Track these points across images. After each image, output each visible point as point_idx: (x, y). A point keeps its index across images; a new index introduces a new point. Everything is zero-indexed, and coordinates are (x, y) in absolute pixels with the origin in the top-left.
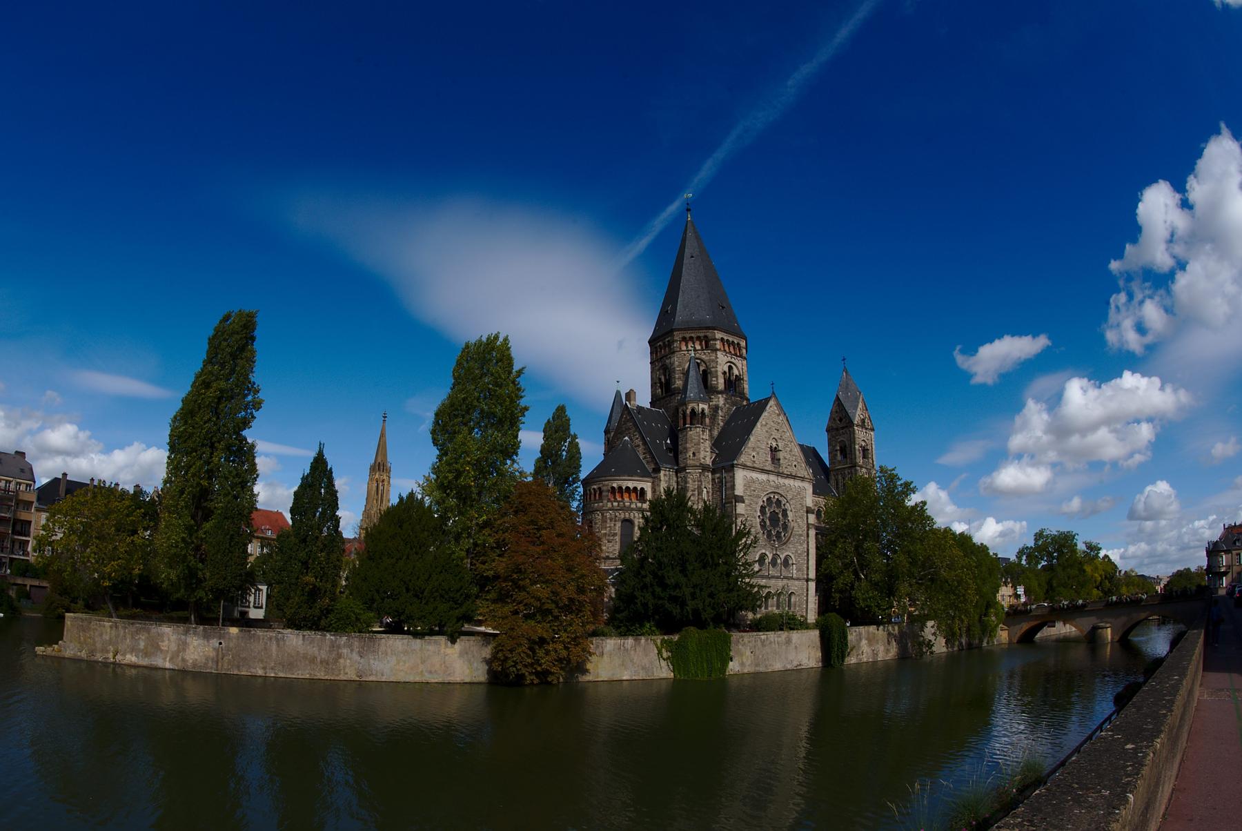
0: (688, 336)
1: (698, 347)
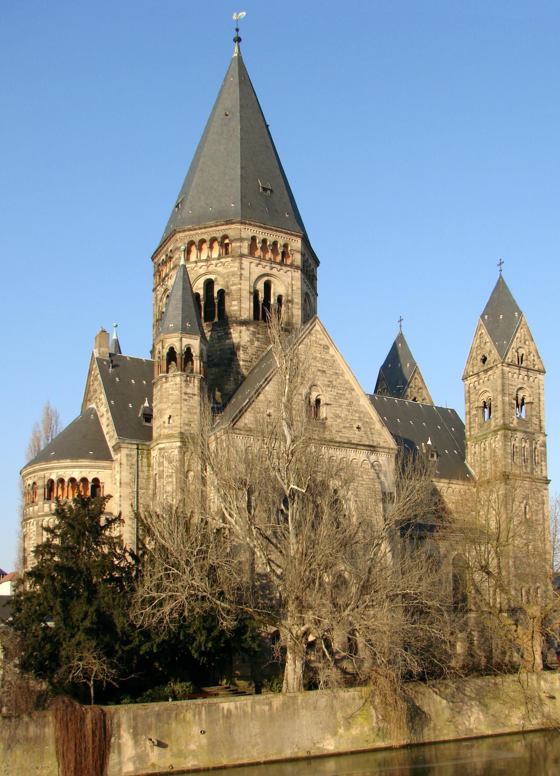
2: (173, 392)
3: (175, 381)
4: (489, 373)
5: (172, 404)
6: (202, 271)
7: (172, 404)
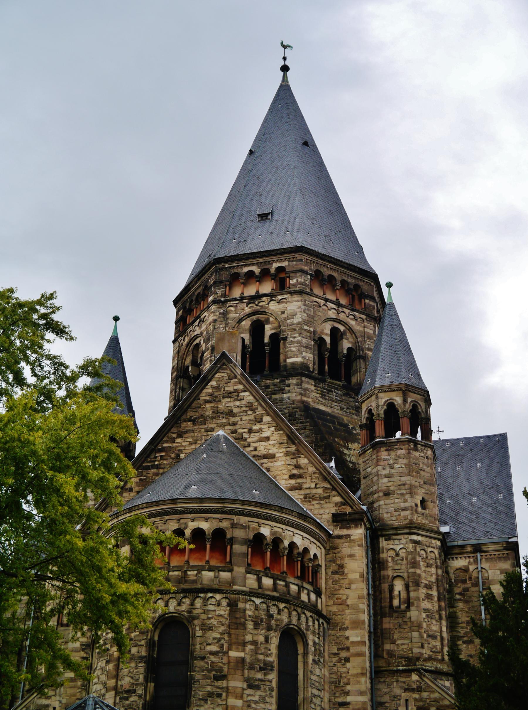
0: (326, 272)
2: (425, 467)
3: (426, 453)
5: (425, 483)
6: (332, 314)
7: (425, 483)
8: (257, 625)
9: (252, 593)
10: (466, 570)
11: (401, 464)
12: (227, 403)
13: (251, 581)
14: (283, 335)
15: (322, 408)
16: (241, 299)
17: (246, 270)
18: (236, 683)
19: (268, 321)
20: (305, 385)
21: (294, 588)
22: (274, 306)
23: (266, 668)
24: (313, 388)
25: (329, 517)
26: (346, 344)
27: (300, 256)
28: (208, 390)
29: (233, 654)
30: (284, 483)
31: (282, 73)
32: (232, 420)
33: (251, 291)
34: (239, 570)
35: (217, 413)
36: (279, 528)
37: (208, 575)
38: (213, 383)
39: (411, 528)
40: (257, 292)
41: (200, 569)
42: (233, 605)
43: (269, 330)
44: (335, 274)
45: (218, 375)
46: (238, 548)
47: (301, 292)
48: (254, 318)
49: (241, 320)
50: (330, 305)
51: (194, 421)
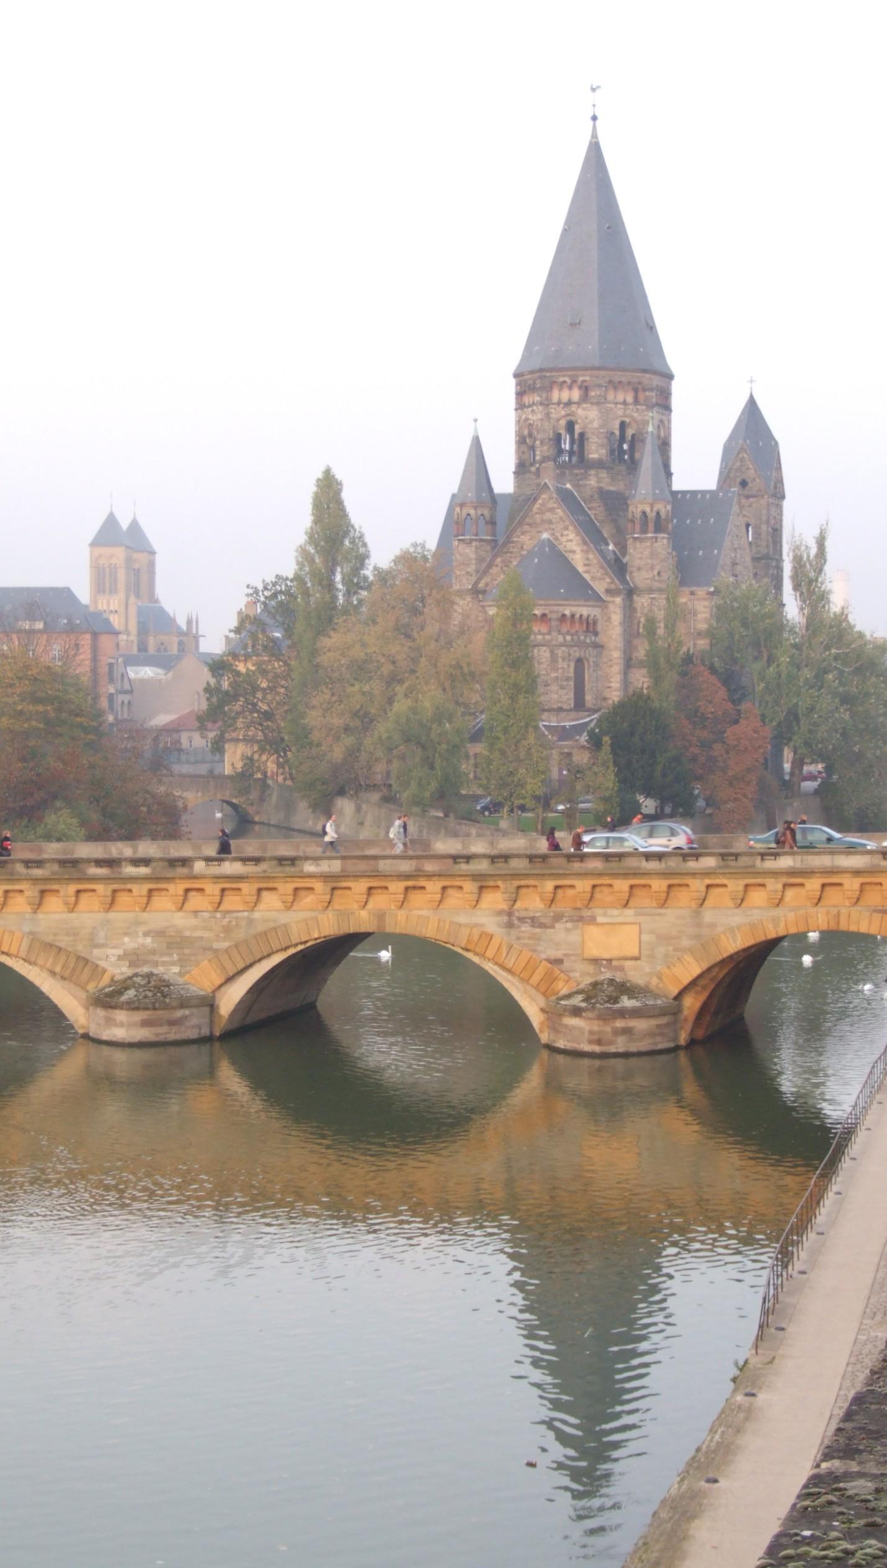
0: (616, 379)
1: (630, 399)
4: (751, 500)
6: (620, 413)
8: (563, 660)
9: (561, 645)
10: (686, 604)
11: (647, 552)
12: (548, 516)
13: (560, 639)
14: (587, 436)
15: (612, 488)
16: (559, 403)
17: (561, 379)
18: (554, 688)
19: (577, 422)
20: (601, 475)
21: (582, 638)
22: (580, 412)
23: (568, 679)
24: (604, 475)
25: (603, 590)
26: (630, 432)
27: (596, 373)
28: (537, 506)
29: (553, 675)
30: (581, 569)
31: (591, 123)
32: (553, 526)
33: (565, 395)
34: (554, 634)
35: (543, 521)
36: (574, 609)
37: (539, 637)
38: (540, 501)
39: (651, 590)
40: (570, 400)
41: (536, 634)
42: (552, 652)
43: (578, 429)
44: (623, 379)
45: (543, 496)
46: (554, 623)
47: (598, 404)
48: (568, 418)
49: (559, 420)
50: (619, 406)
51: (530, 525)
